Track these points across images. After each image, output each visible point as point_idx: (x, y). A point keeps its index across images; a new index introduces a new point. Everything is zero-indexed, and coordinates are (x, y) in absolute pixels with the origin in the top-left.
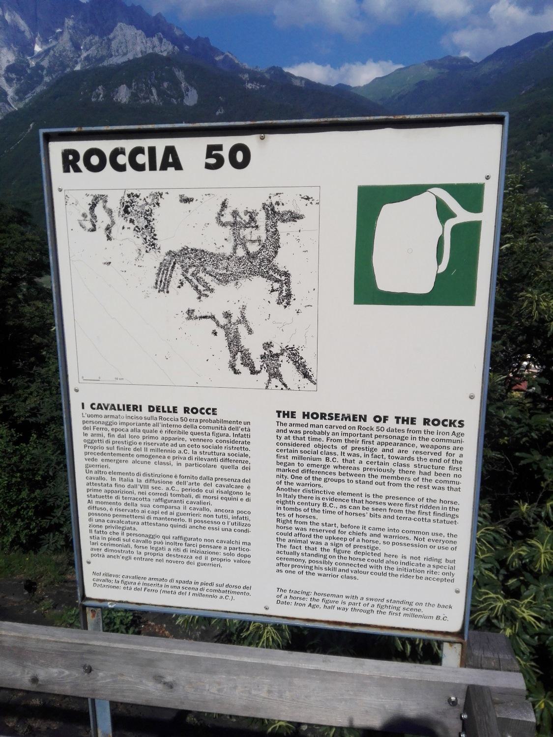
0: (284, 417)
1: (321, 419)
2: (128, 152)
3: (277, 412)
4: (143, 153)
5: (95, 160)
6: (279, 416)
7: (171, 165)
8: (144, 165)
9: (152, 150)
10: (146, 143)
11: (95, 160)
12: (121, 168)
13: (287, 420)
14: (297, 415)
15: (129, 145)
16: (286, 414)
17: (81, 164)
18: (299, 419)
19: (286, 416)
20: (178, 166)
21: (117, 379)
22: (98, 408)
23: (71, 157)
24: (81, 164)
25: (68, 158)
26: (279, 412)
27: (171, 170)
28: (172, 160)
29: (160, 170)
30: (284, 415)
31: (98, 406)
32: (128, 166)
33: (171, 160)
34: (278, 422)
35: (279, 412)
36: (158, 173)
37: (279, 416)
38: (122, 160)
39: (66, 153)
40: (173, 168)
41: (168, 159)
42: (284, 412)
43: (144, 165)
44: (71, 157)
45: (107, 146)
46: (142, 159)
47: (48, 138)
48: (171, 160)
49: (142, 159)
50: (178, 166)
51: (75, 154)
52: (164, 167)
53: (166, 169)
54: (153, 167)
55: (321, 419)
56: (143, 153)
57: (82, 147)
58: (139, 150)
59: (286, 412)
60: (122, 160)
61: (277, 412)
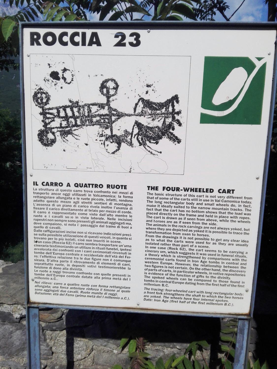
0: (151, 190)
1: (177, 191)
2: (69, 35)
3: (148, 187)
4: (79, 36)
6: (149, 189)
7: (94, 43)
8: (79, 42)
9: (84, 35)
10: (80, 31)
11: (50, 39)
12: (65, 44)
14: (159, 188)
15: (70, 31)
17: (41, 41)
18: (160, 191)
20: (99, 44)
22: (46, 185)
23: (35, 37)
24: (41, 41)
25: (34, 37)
26: (149, 187)
27: (94, 46)
28: (95, 41)
30: (152, 188)
32: (69, 43)
33: (94, 40)
34: (148, 193)
35: (149, 187)
36: (87, 47)
38: (66, 39)
39: (32, 34)
40: (96, 45)
43: (79, 42)
44: (35, 37)
46: (78, 39)
47: (24, 26)
48: (94, 40)
49: (78, 39)
50: (99, 44)
51: (38, 35)
52: (90, 44)
54: (84, 44)
55: (177, 191)
56: (79, 36)
57: (42, 31)
60: (66, 39)
61: (148, 187)
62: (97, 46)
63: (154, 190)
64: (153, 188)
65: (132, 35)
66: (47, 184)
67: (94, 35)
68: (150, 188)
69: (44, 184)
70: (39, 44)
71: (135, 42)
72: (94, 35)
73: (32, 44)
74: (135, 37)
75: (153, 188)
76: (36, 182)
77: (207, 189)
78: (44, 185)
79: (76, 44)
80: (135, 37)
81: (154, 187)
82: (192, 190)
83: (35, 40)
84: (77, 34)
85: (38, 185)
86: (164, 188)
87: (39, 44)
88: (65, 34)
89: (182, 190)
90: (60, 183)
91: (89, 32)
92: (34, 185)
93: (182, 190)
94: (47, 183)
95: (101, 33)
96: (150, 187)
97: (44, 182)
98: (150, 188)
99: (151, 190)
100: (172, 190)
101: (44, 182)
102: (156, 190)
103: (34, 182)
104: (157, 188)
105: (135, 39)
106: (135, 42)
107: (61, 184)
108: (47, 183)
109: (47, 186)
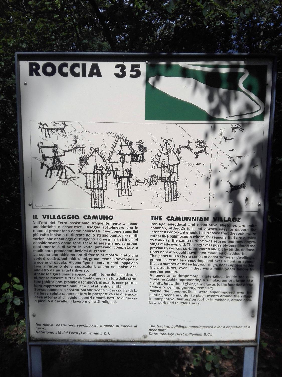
0: (155, 220)
3: (151, 217)
4: (79, 67)
6: (152, 220)
9: (84, 66)
10: (81, 63)
12: (65, 75)
13: (158, 222)
14: (163, 218)
15: (70, 63)
16: (156, 218)
19: (156, 219)
20: (99, 75)
22: (171, 220)
26: (152, 217)
27: (95, 77)
29: (89, 76)
31: (228, 219)
33: (95, 71)
35: (152, 217)
36: (87, 78)
37: (152, 220)
38: (65, 70)
41: (94, 71)
42: (155, 217)
45: (57, 64)
46: (78, 70)
48: (95, 71)
49: (78, 70)
50: (99, 75)
52: (91, 75)
53: (92, 77)
54: (84, 75)
56: (79, 67)
59: (156, 217)
60: (65, 70)
61: (151, 217)
62: (98, 77)
63: (158, 220)
64: (156, 218)
66: (172, 219)
67: (95, 66)
68: (154, 218)
69: (86, 217)
75: (156, 218)
76: (36, 216)
78: (86, 219)
79: (77, 75)
81: (158, 217)
84: (78, 65)
85: (38, 218)
90: (110, 216)
91: (89, 65)
92: (34, 218)
94: (59, 216)
95: (102, 65)
96: (153, 217)
97: (86, 216)
98: (154, 218)
99: (155, 220)
101: (86, 216)
102: (160, 220)
103: (34, 216)
104: (160, 218)
107: (111, 218)
108: (59, 216)
109: (59, 219)
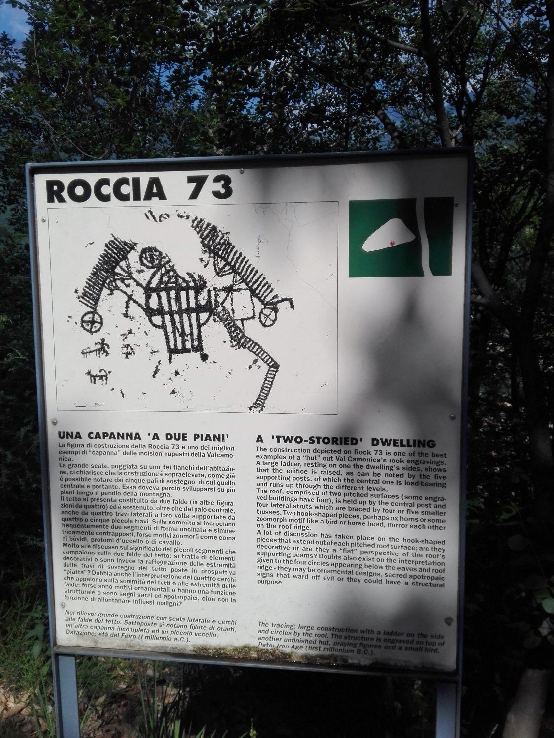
2: (112, 183)
4: (128, 184)
5: (79, 191)
7: (155, 195)
9: (137, 182)
10: (130, 176)
11: (79, 191)
12: (106, 198)
15: (114, 177)
17: (65, 194)
21: (97, 404)
23: (55, 188)
27: (155, 200)
28: (156, 191)
32: (113, 197)
33: (155, 190)
38: (106, 190)
39: (50, 184)
44: (55, 188)
45: (92, 178)
46: (126, 189)
47: (34, 171)
48: (155, 190)
49: (126, 189)
50: (162, 196)
52: (148, 197)
53: (150, 199)
54: (137, 197)
56: (128, 184)
57: (67, 179)
58: (125, 181)
60: (106, 190)
62: (160, 199)
65: (217, 179)
67: (155, 182)
70: (61, 200)
71: (223, 191)
72: (155, 182)
73: (50, 200)
74: (222, 182)
77: (214, 436)
79: (125, 198)
80: (222, 182)
82: (121, 436)
83: (54, 193)
84: (125, 181)
86: (196, 437)
87: (61, 200)
88: (106, 182)
89: (306, 441)
91: (145, 178)
93: (306, 441)
95: (167, 178)
100: (175, 439)
105: (223, 187)
106: (223, 191)
